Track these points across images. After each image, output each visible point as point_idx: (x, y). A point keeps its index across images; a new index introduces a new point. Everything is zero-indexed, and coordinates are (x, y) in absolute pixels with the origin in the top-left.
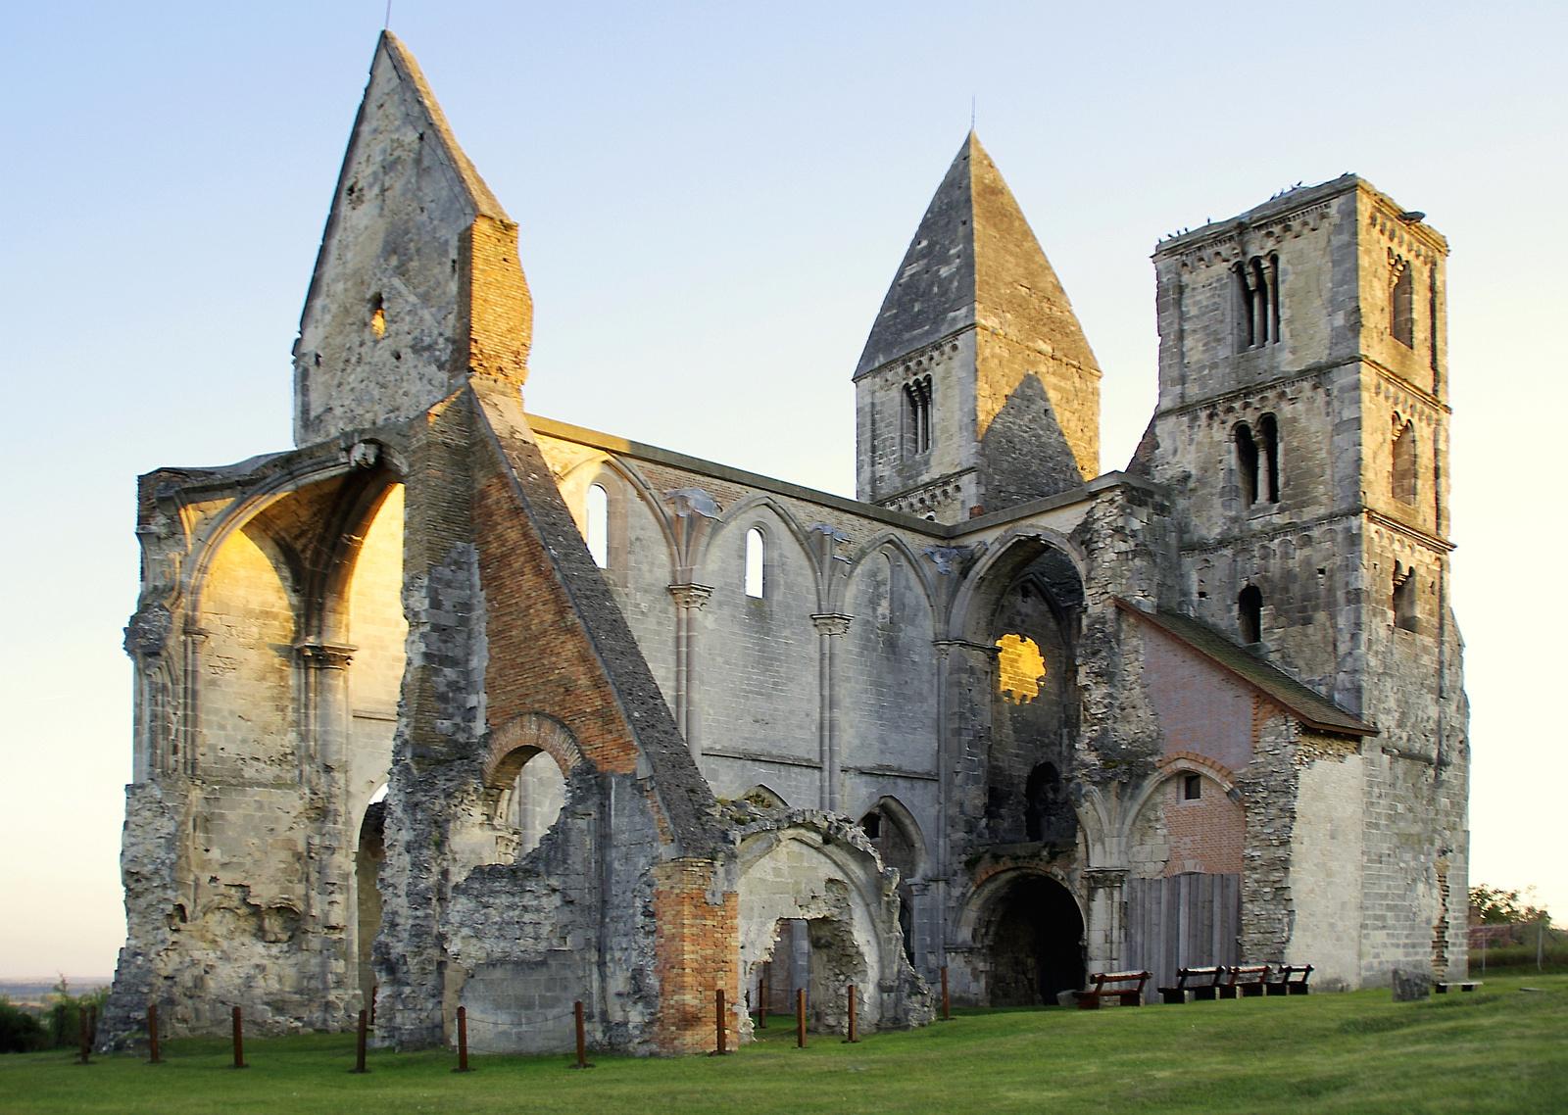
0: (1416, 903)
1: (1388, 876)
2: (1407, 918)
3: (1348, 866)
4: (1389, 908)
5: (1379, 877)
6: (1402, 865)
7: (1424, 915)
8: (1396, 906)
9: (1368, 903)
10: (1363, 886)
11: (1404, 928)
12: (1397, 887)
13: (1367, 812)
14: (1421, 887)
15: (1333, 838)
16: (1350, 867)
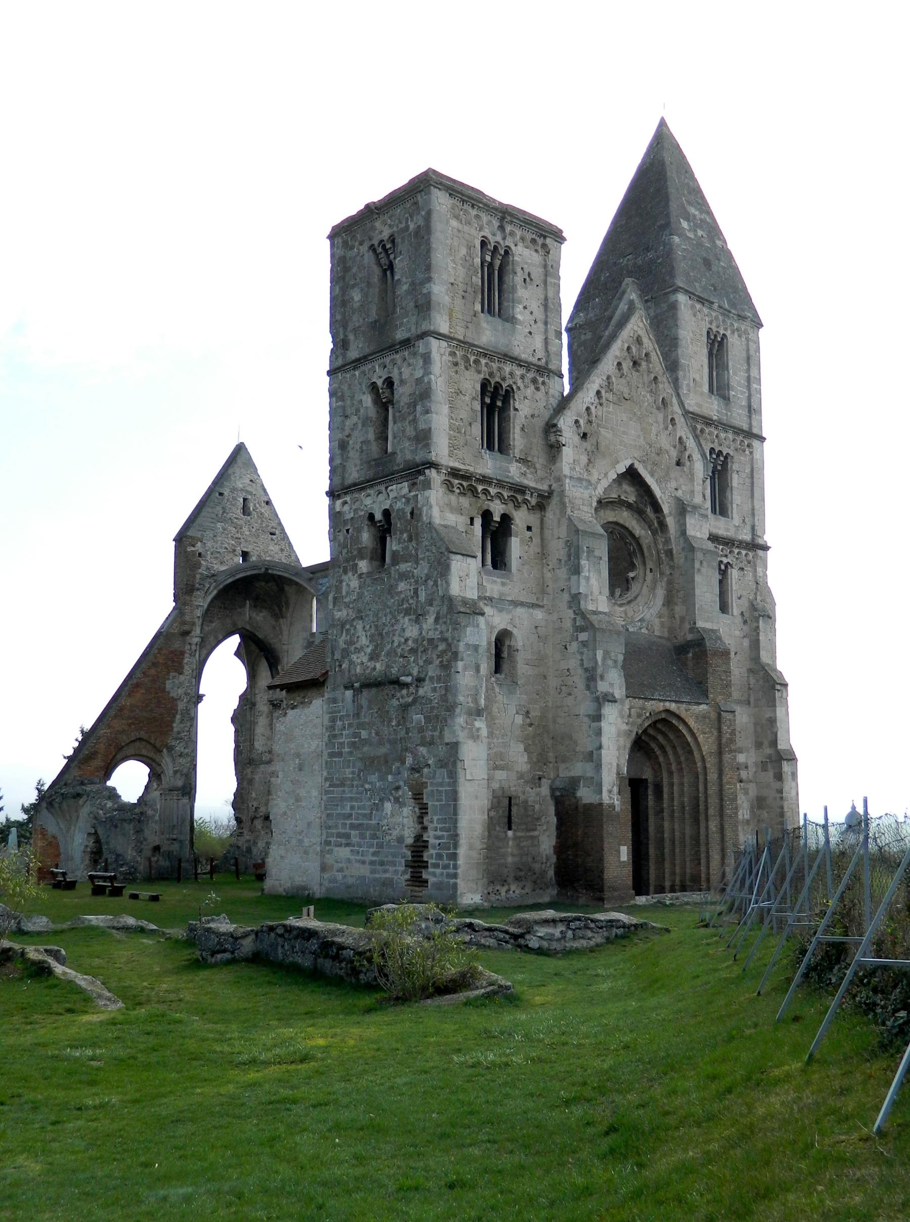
0: (385, 822)
1: (351, 798)
2: (374, 836)
3: (312, 789)
4: (353, 827)
5: (342, 799)
6: (367, 786)
7: (395, 833)
8: (360, 825)
9: (330, 823)
10: (326, 808)
11: (372, 846)
12: (363, 807)
13: (330, 743)
14: (388, 806)
15: (300, 770)
16: (315, 793)
